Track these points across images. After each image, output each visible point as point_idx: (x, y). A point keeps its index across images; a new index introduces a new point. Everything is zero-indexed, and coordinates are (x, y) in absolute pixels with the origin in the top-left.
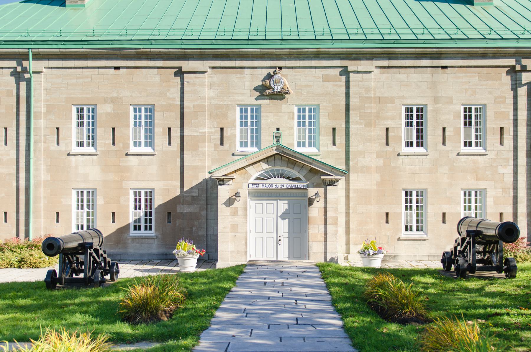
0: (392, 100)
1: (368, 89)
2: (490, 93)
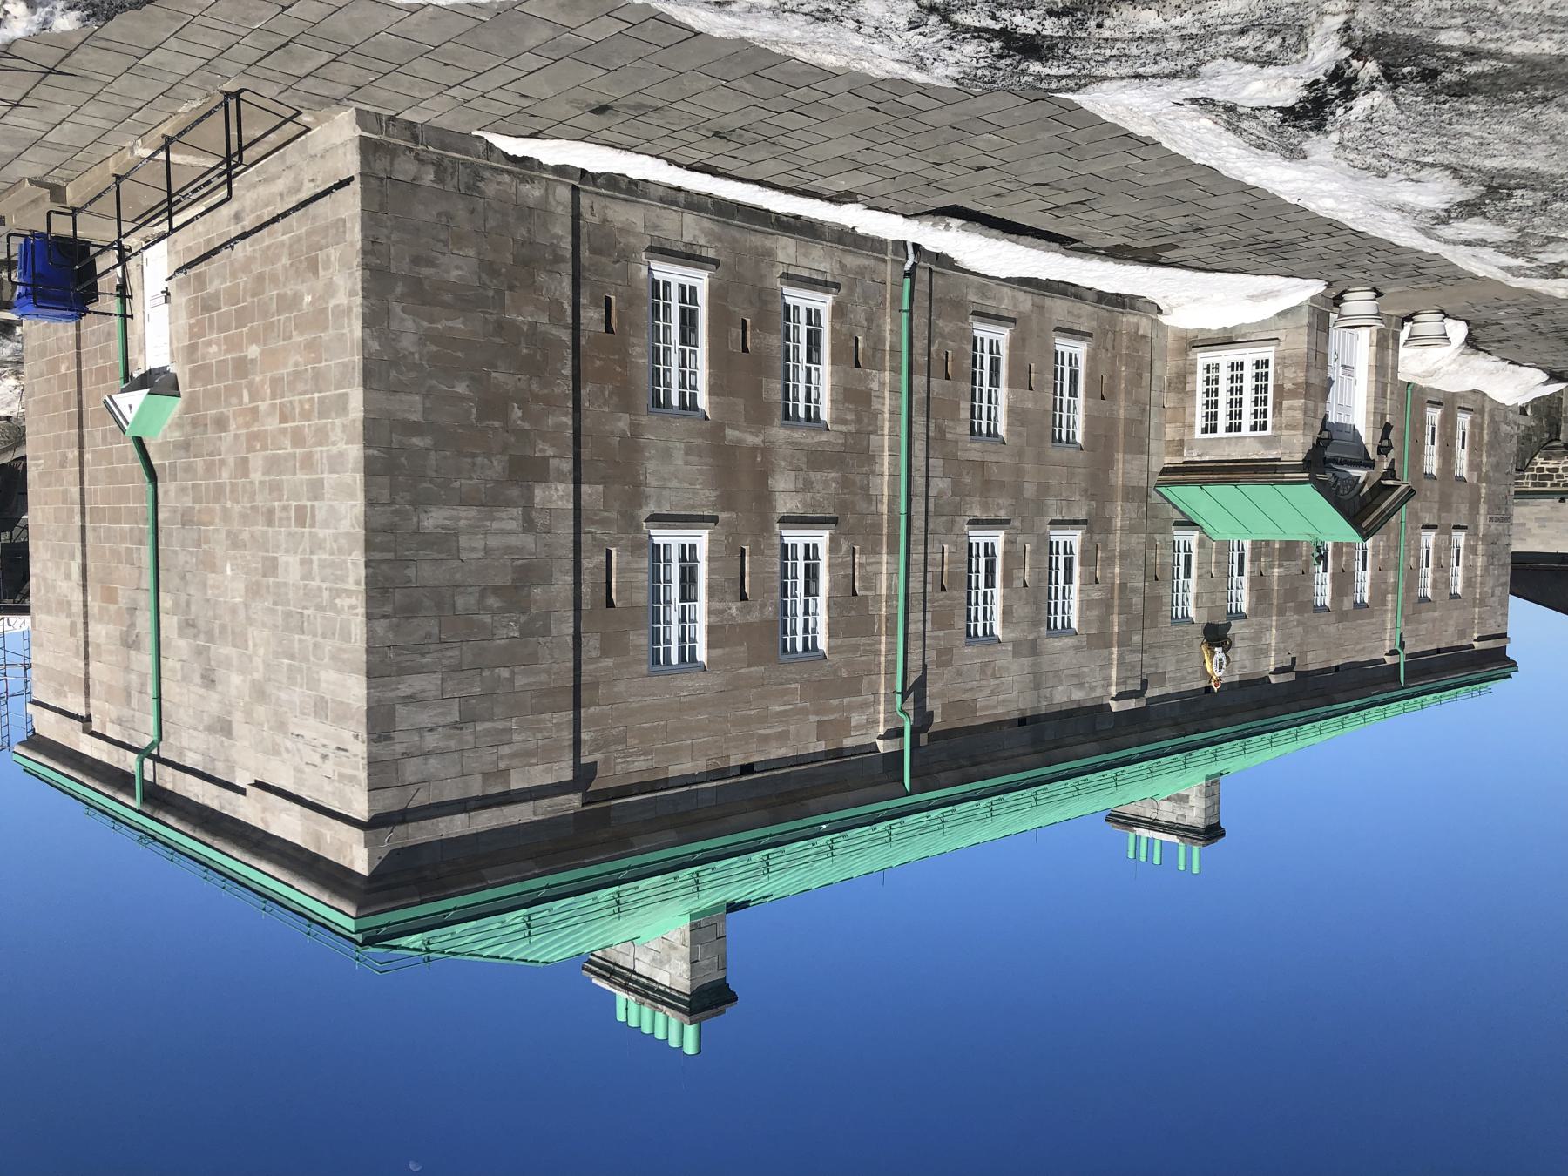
2: (959, 673)
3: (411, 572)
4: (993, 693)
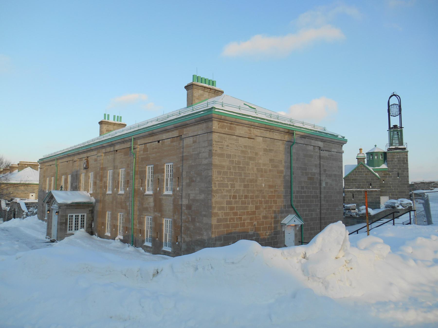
3: (206, 185)
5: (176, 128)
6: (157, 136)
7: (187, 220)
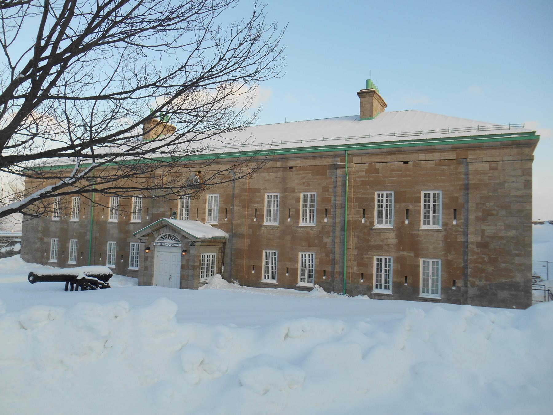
0: (258, 190)
1: (244, 184)
2: (319, 184)
3: (519, 220)
4: (304, 178)
5: (454, 149)
6: (405, 156)
7: (479, 260)
